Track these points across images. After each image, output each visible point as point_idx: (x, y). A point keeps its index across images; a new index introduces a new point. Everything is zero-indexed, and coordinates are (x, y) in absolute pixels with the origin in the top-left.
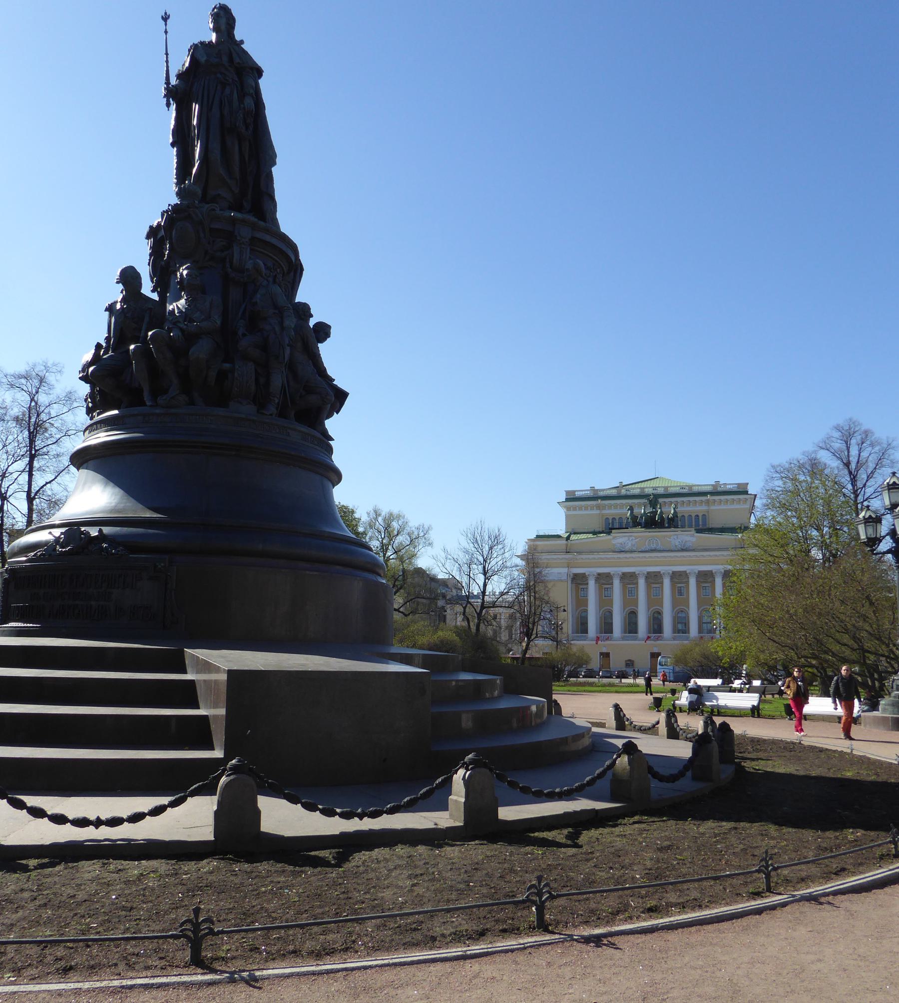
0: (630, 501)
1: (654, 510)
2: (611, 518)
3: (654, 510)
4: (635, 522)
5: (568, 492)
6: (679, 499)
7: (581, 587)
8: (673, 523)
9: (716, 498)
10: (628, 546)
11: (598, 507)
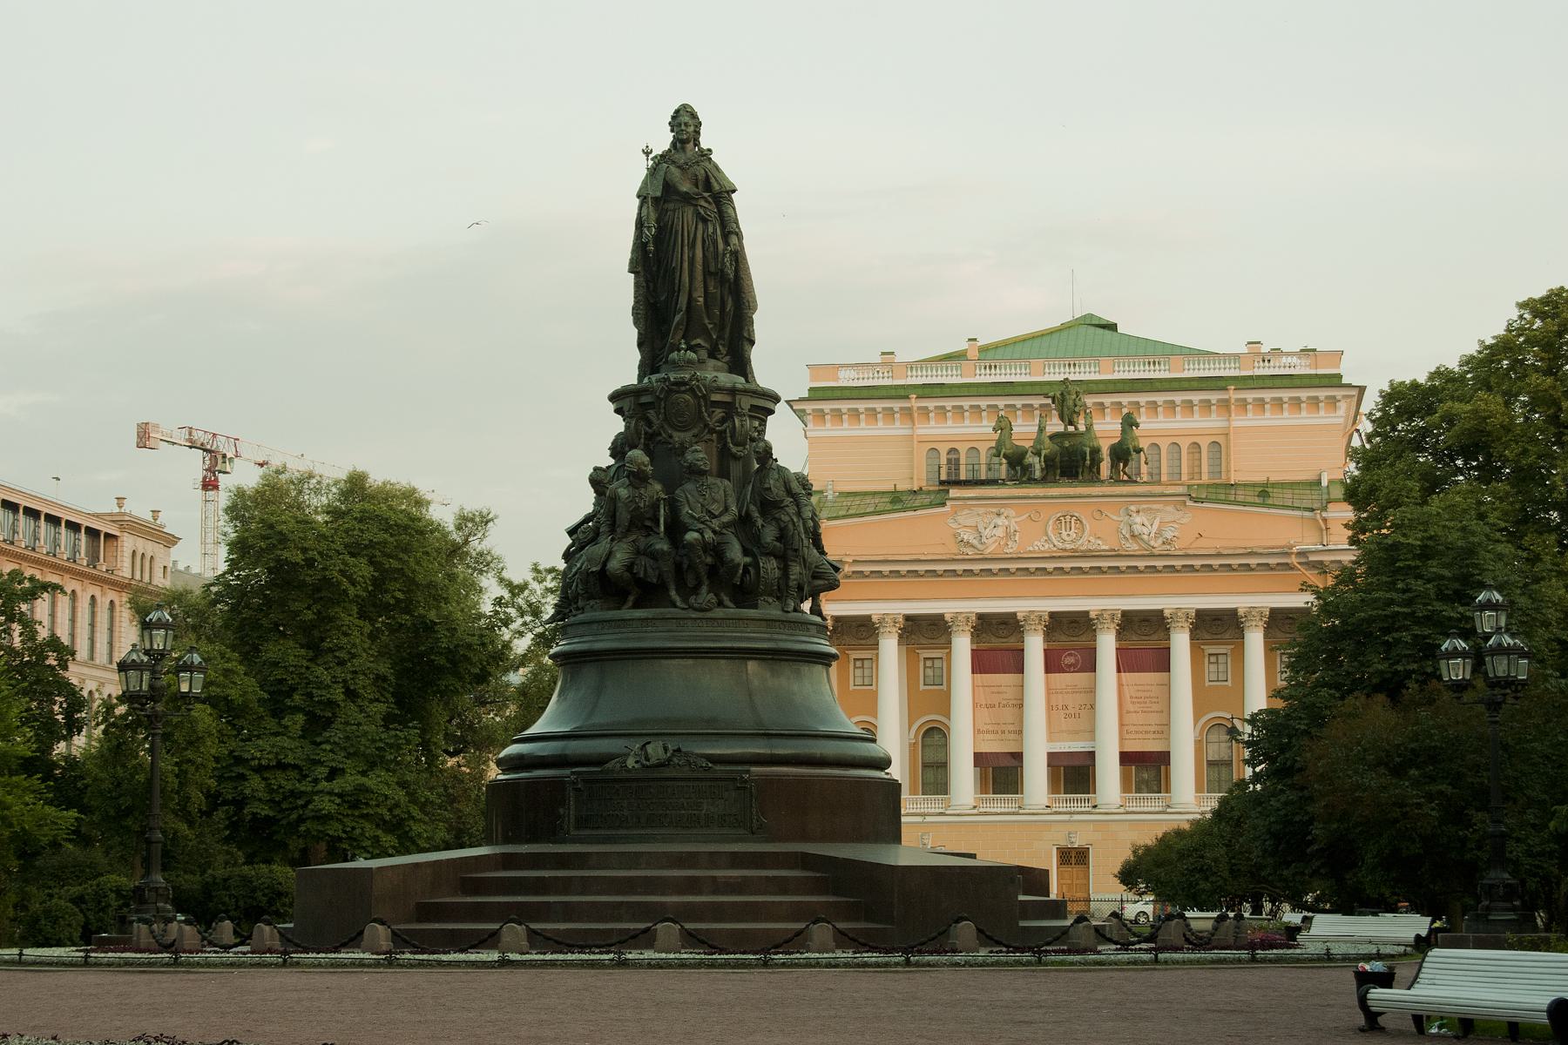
1: (1071, 429)
2: (944, 449)
3: (1071, 429)
4: (1017, 466)
7: (854, 655)
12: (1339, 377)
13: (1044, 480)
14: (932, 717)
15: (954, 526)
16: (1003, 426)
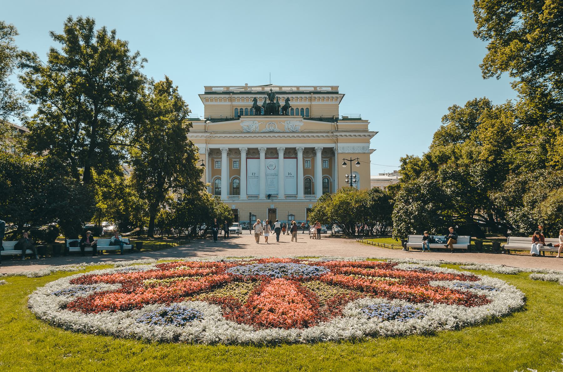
0: (254, 96)
2: (239, 109)
5: (206, 87)
6: (290, 96)
7: (215, 160)
8: (286, 110)
9: (316, 96)
10: (253, 129)
11: (231, 100)
12: (338, 92)
13: (264, 115)
14: (235, 176)
15: (242, 125)
16: (255, 100)
